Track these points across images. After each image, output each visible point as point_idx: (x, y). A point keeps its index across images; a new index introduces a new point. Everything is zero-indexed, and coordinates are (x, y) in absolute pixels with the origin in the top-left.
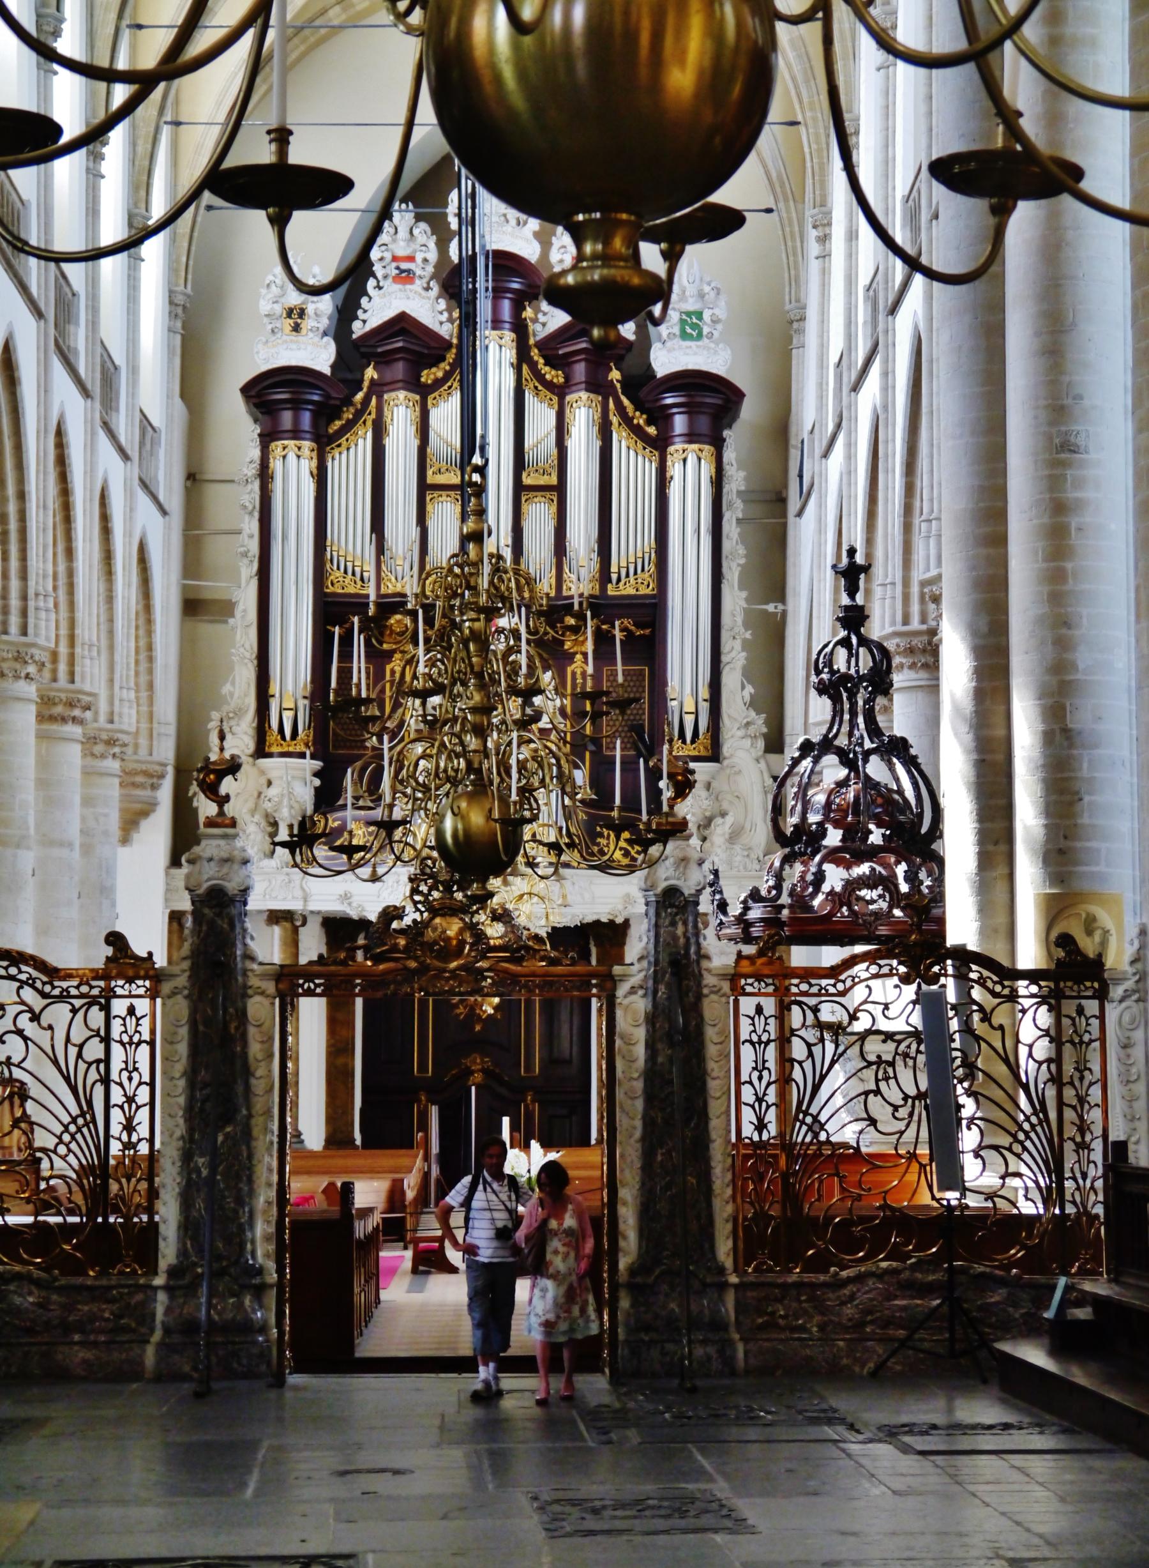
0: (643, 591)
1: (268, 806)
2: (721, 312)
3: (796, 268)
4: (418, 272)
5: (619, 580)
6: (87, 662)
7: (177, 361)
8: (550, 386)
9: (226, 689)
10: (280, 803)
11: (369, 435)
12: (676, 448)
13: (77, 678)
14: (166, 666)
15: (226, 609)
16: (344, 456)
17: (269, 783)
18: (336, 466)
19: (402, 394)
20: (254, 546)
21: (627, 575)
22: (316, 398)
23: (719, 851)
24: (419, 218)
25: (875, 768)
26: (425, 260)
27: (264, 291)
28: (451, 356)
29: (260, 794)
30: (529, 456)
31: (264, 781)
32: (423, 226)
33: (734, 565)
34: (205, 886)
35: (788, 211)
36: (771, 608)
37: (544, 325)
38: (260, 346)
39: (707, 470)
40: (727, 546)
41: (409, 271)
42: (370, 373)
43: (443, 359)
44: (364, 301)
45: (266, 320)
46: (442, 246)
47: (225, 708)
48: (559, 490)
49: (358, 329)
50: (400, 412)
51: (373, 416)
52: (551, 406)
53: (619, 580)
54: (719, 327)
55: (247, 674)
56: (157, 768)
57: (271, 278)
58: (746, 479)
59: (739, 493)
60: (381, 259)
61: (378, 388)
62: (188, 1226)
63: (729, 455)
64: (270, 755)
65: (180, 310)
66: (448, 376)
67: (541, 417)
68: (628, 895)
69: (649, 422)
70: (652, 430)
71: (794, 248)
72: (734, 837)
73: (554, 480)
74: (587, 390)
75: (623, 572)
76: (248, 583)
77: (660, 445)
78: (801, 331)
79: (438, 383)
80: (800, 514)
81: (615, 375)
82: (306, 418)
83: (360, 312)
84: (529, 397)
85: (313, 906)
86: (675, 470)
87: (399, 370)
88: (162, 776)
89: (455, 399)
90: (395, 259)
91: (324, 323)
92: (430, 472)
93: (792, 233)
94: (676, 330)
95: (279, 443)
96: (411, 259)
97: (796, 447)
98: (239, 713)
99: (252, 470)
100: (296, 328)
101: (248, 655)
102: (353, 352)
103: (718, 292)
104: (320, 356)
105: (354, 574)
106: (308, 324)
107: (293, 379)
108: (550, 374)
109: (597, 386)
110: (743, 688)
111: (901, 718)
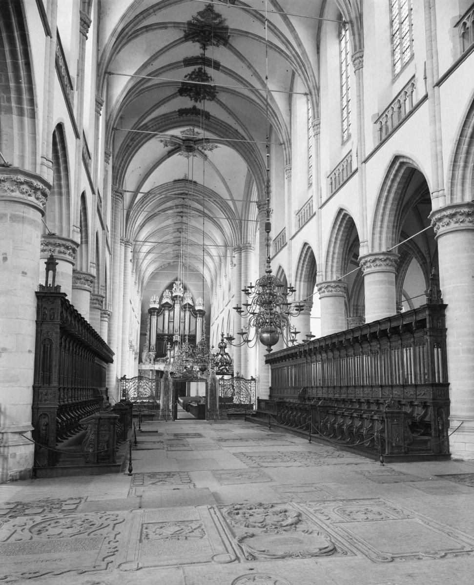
12: (198, 318)
15: (146, 335)
25: (225, 356)
48: (185, 322)
50: (167, 313)
55: (148, 342)
61: (164, 310)
62: (164, 405)
77: (196, 318)
82: (156, 313)
87: (167, 308)
104: (157, 306)
107: (154, 309)
109: (190, 311)
111: (227, 350)
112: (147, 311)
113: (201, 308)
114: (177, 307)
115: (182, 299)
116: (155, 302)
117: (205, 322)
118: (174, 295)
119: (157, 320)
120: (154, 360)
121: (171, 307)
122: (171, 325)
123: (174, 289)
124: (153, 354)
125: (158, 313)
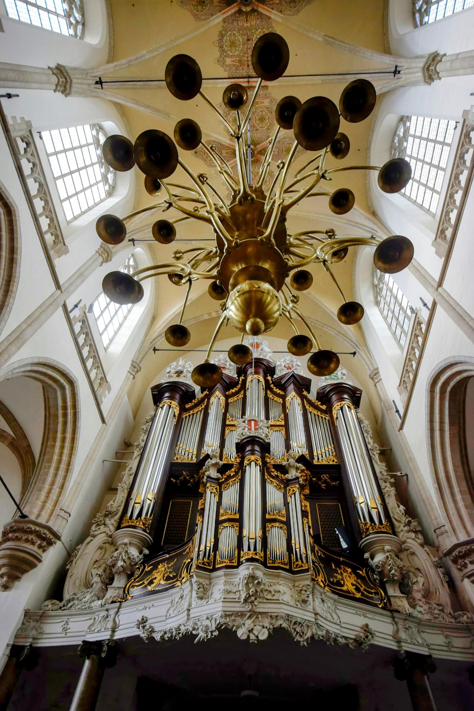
0: (331, 463)
5: (318, 459)
12: (336, 406)
14: (78, 484)
21: (322, 457)
23: (421, 603)
28: (239, 386)
33: (375, 453)
51: (205, 404)
56: (49, 535)
68: (367, 625)
69: (322, 404)
70: (324, 407)
72: (427, 595)
73: (283, 423)
85: (118, 636)
88: (50, 543)
108: (278, 391)
110: (399, 507)
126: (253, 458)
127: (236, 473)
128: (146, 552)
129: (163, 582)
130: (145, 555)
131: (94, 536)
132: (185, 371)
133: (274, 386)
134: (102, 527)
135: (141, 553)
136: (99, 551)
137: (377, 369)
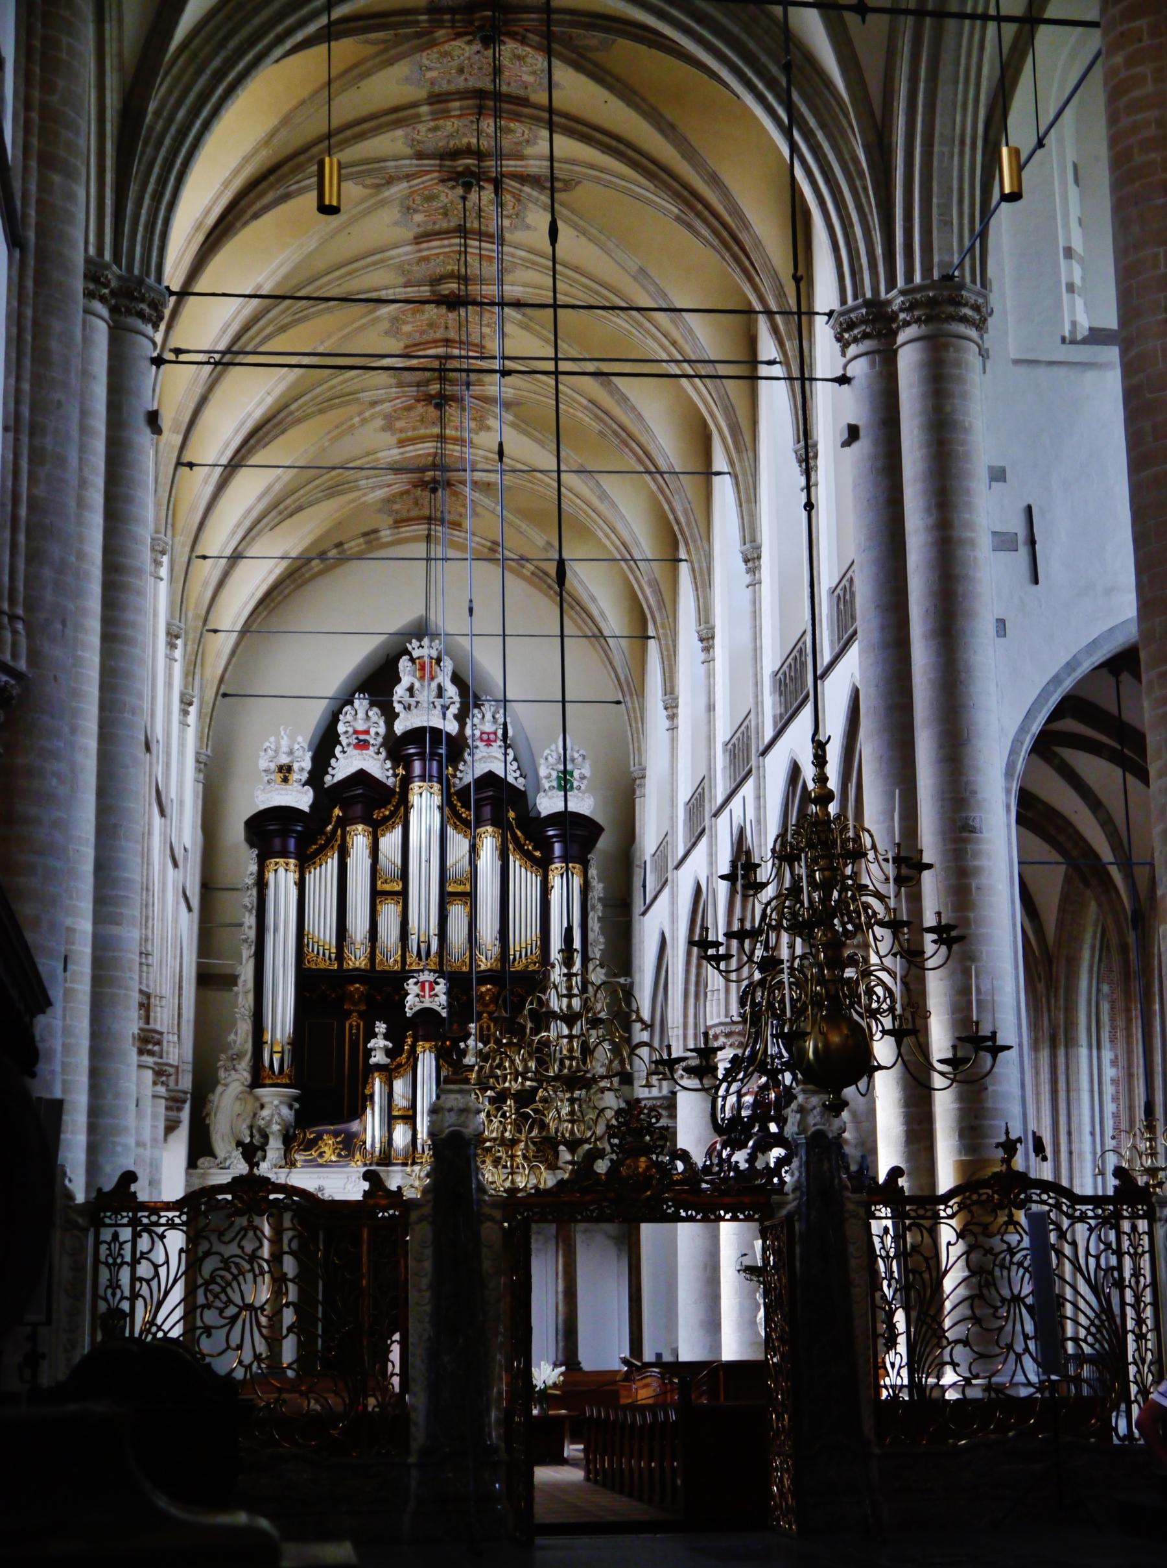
1: (262, 1123)
2: (586, 771)
3: (639, 742)
4: (372, 741)
6: (159, 1009)
7: (200, 802)
8: (466, 823)
9: (232, 1037)
10: (270, 1122)
11: (336, 856)
13: (151, 1021)
15: (231, 980)
16: (318, 870)
17: (262, 1107)
18: (312, 878)
19: (360, 827)
20: (252, 934)
21: (520, 956)
22: (299, 828)
24: (372, 704)
26: (377, 734)
27: (262, 753)
28: (394, 801)
29: (255, 1115)
30: (450, 872)
31: (257, 1105)
32: (375, 709)
33: (596, 950)
34: (447, 1131)
35: (633, 703)
36: (622, 980)
37: (461, 779)
38: (259, 792)
39: (577, 882)
40: (591, 936)
41: (365, 741)
42: (337, 812)
43: (389, 803)
44: (333, 761)
45: (263, 774)
46: (390, 724)
47: (230, 1052)
48: (470, 897)
49: (328, 780)
50: (359, 841)
52: (465, 836)
53: (514, 959)
54: (585, 782)
55: (244, 1028)
56: (181, 1095)
57: (267, 744)
58: (604, 888)
59: (600, 899)
60: (346, 732)
61: (343, 823)
63: (593, 872)
64: (264, 1086)
65: (202, 766)
66: (393, 814)
67: (459, 845)
69: (535, 849)
70: (538, 854)
71: (637, 728)
74: (492, 825)
75: (518, 954)
76: (247, 961)
78: (642, 786)
79: (386, 819)
80: (644, 913)
81: (512, 814)
82: (292, 843)
83: (330, 769)
84: (450, 831)
86: (556, 882)
87: (358, 809)
88: (184, 1102)
89: (398, 830)
90: (356, 732)
91: (305, 776)
92: (379, 883)
93: (636, 718)
94: (555, 784)
95: (273, 860)
96: (367, 732)
97: (639, 867)
98: (240, 1056)
99: (250, 881)
100: (285, 780)
101: (247, 1013)
102: (328, 797)
103: (584, 757)
104: (301, 799)
105: (324, 954)
106: (295, 776)
109: (498, 822)
112: (235, 832)
113: (582, 804)
114: (425, 807)
115: (457, 748)
116: (285, 771)
117: (598, 889)
118: (399, 727)
119: (301, 885)
120: (288, 1140)
121: (377, 804)
122: (390, 913)
123: (400, 691)
124: (276, 1105)
125: (304, 841)
126: (427, 1045)
127: (408, 1058)
128: (297, 1106)
129: (334, 1158)
130: (296, 1111)
131: (226, 1085)
132: (296, 766)
133: (459, 800)
134: (233, 1072)
135: (291, 1107)
136: (238, 1103)
137: (645, 769)
